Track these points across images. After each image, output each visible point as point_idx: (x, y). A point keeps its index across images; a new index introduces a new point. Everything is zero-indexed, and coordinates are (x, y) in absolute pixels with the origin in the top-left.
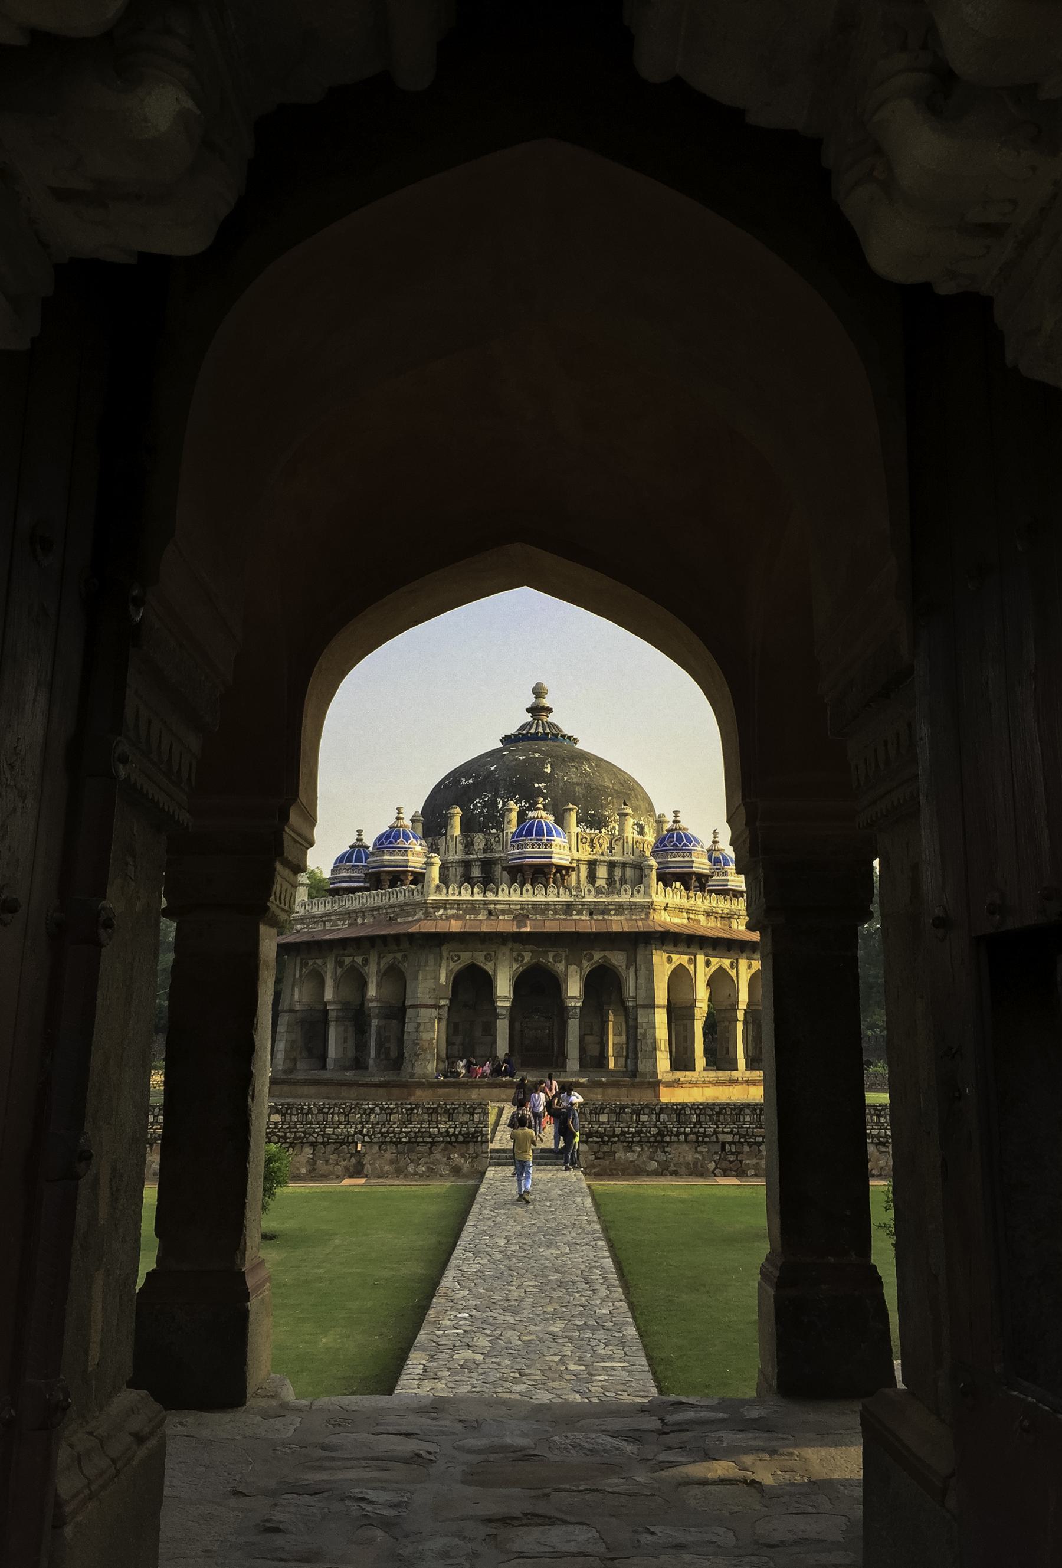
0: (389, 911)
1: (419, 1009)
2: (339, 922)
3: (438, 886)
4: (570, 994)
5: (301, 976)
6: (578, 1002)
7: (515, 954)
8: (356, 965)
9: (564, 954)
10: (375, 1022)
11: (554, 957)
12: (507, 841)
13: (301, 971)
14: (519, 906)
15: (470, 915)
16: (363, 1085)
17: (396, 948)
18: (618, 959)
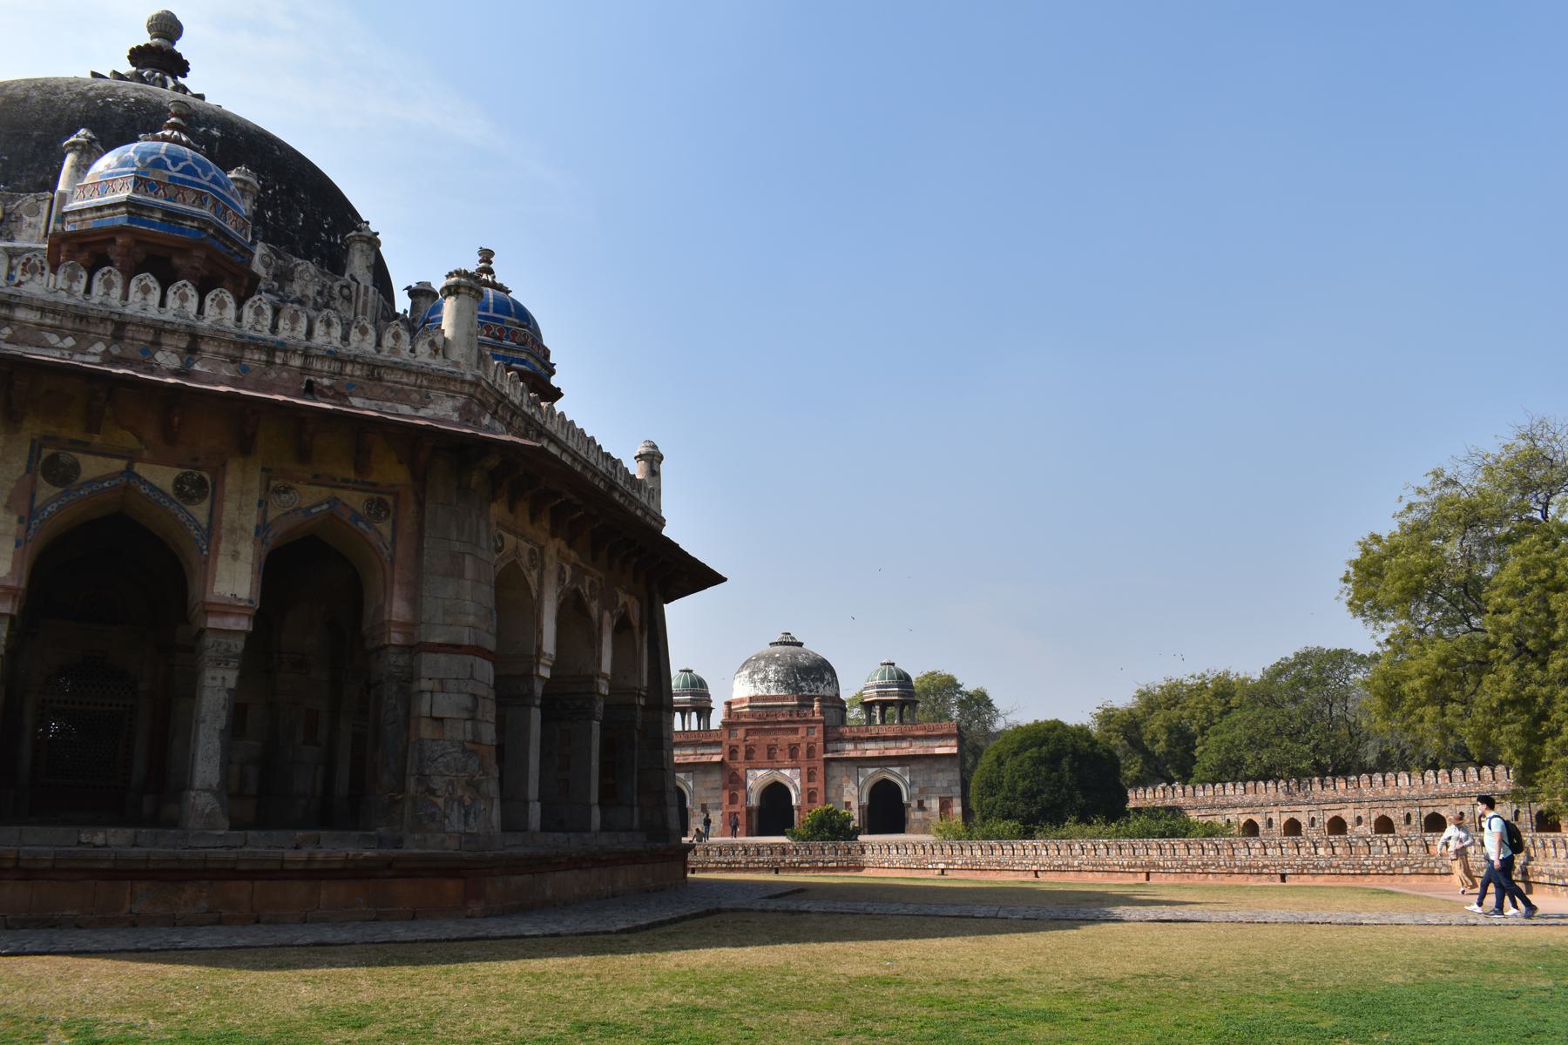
0: (317, 365)
1: (470, 659)
2: (53, 339)
8: (144, 490)
17: (352, 475)
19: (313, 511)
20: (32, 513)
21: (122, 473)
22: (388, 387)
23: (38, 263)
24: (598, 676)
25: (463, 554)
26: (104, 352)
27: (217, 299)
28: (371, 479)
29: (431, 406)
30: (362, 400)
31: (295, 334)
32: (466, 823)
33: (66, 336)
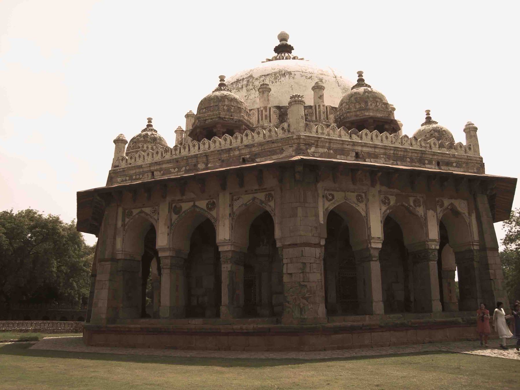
0: (243, 152)
1: (301, 249)
2: (172, 170)
3: (307, 125)
4: (430, 238)
5: (124, 225)
6: (437, 246)
7: (382, 196)
8: (198, 210)
9: (421, 200)
10: (226, 268)
11: (415, 201)
12: (320, 112)
13: (123, 220)
14: (382, 151)
15: (340, 155)
16: (227, 334)
17: (257, 187)
18: (462, 206)
19: (248, 203)
20: (171, 225)
21: (192, 206)
22: (268, 151)
23: (168, 149)
24: (428, 242)
25: (297, 207)
26: (185, 170)
27: (214, 140)
28: (265, 187)
29: (284, 153)
30: (259, 159)
31: (226, 145)
32: (301, 314)
33: (175, 168)
